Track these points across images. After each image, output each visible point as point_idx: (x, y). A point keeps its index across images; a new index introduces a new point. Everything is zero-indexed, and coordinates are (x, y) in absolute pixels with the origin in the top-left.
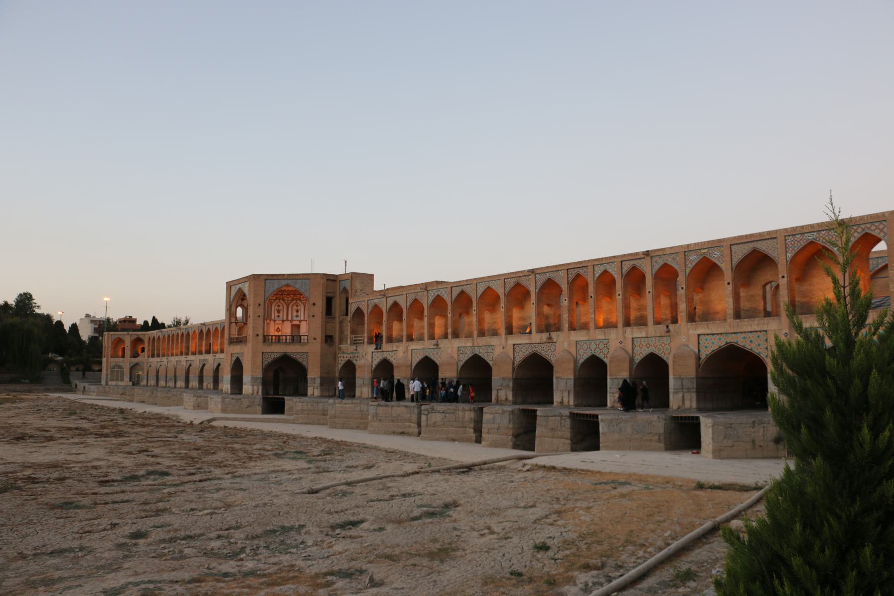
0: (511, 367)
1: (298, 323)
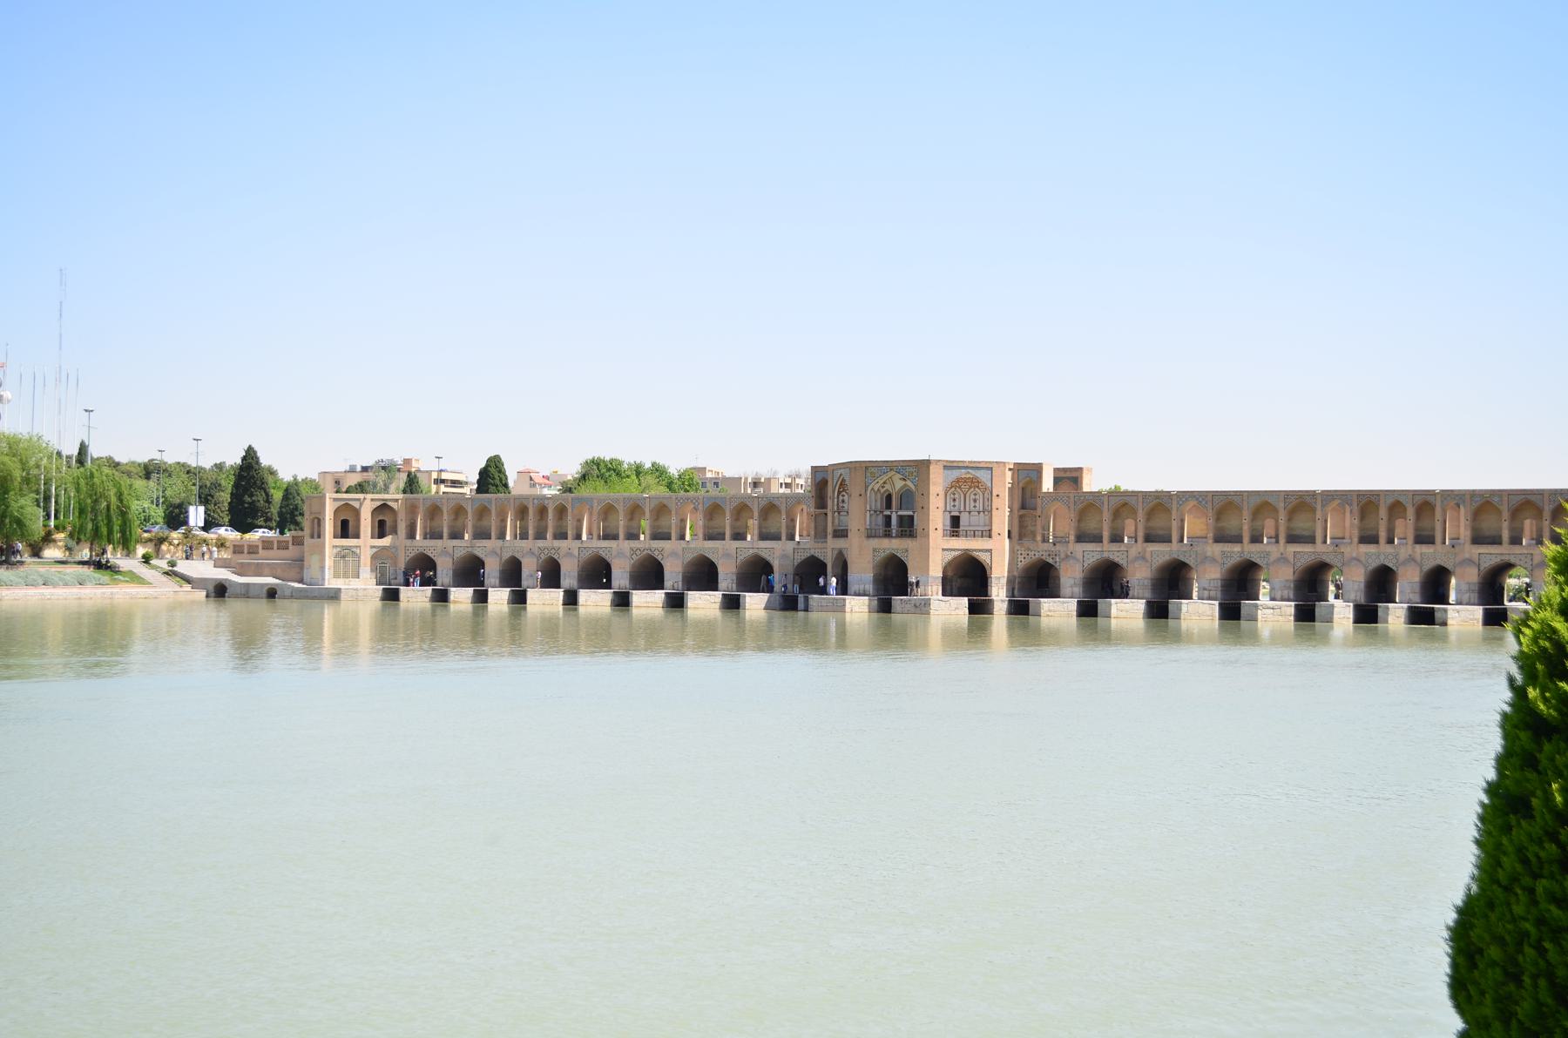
0: (1292, 570)
1: (957, 514)
